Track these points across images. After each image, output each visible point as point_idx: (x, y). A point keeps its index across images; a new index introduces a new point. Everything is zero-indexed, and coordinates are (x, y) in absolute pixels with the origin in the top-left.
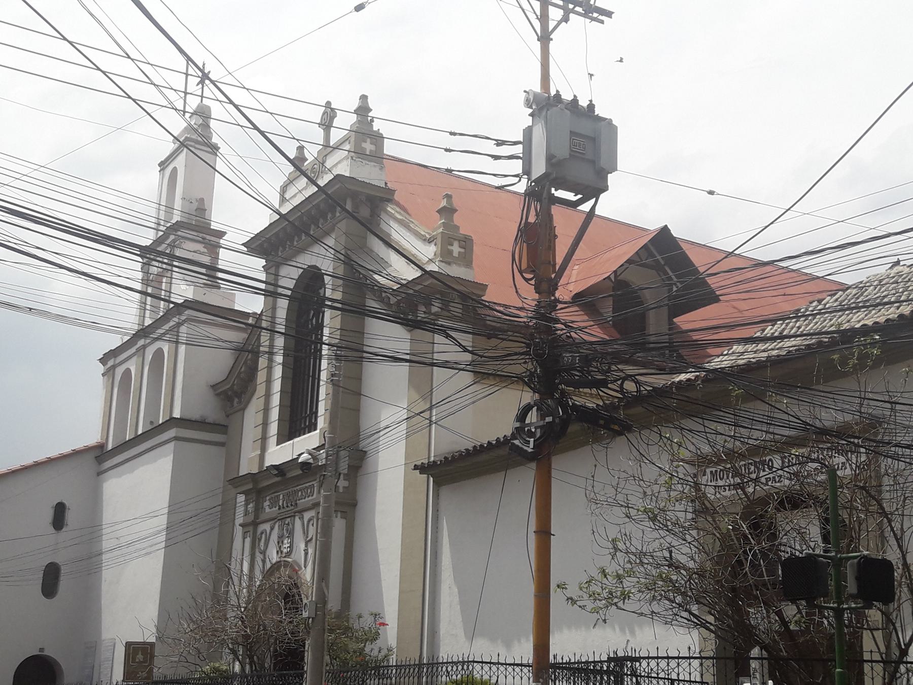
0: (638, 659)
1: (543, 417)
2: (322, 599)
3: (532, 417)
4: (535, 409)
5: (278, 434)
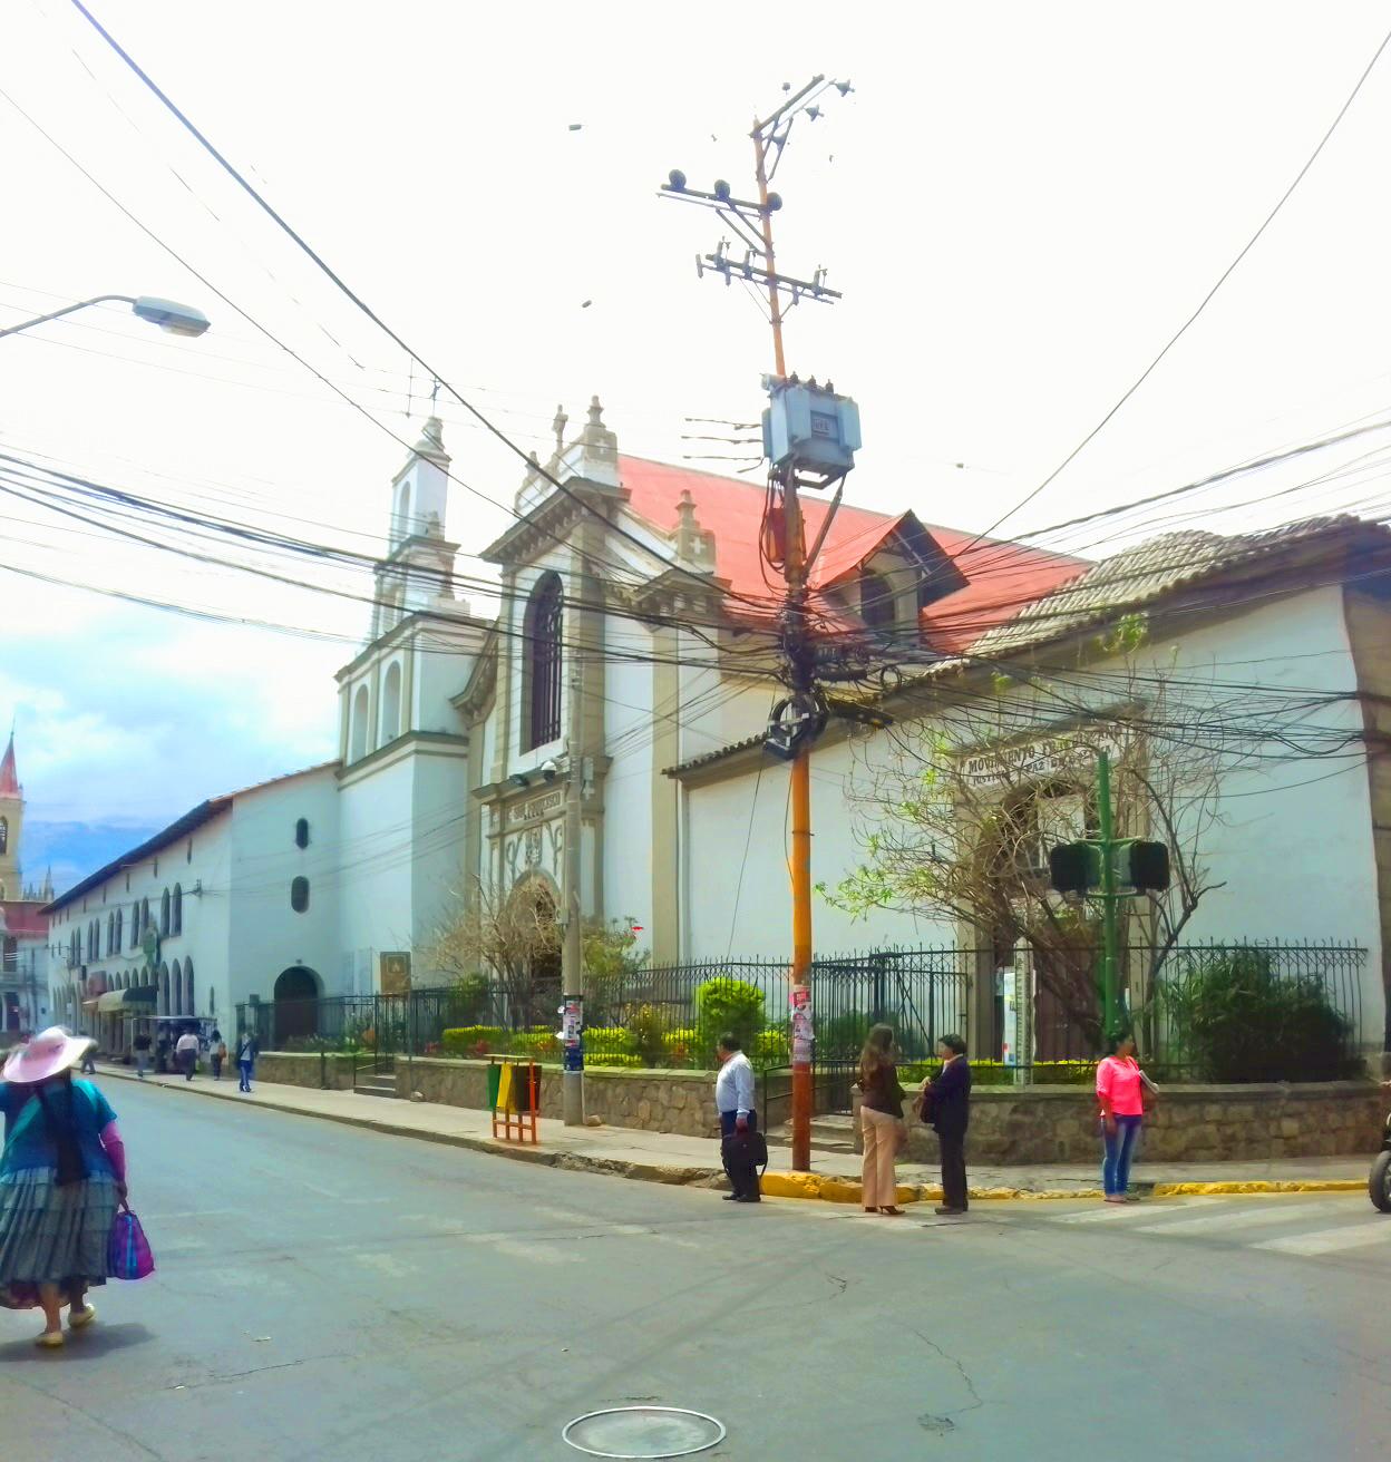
0: (899, 956)
1: (799, 715)
2: (575, 907)
3: (788, 715)
4: (790, 705)
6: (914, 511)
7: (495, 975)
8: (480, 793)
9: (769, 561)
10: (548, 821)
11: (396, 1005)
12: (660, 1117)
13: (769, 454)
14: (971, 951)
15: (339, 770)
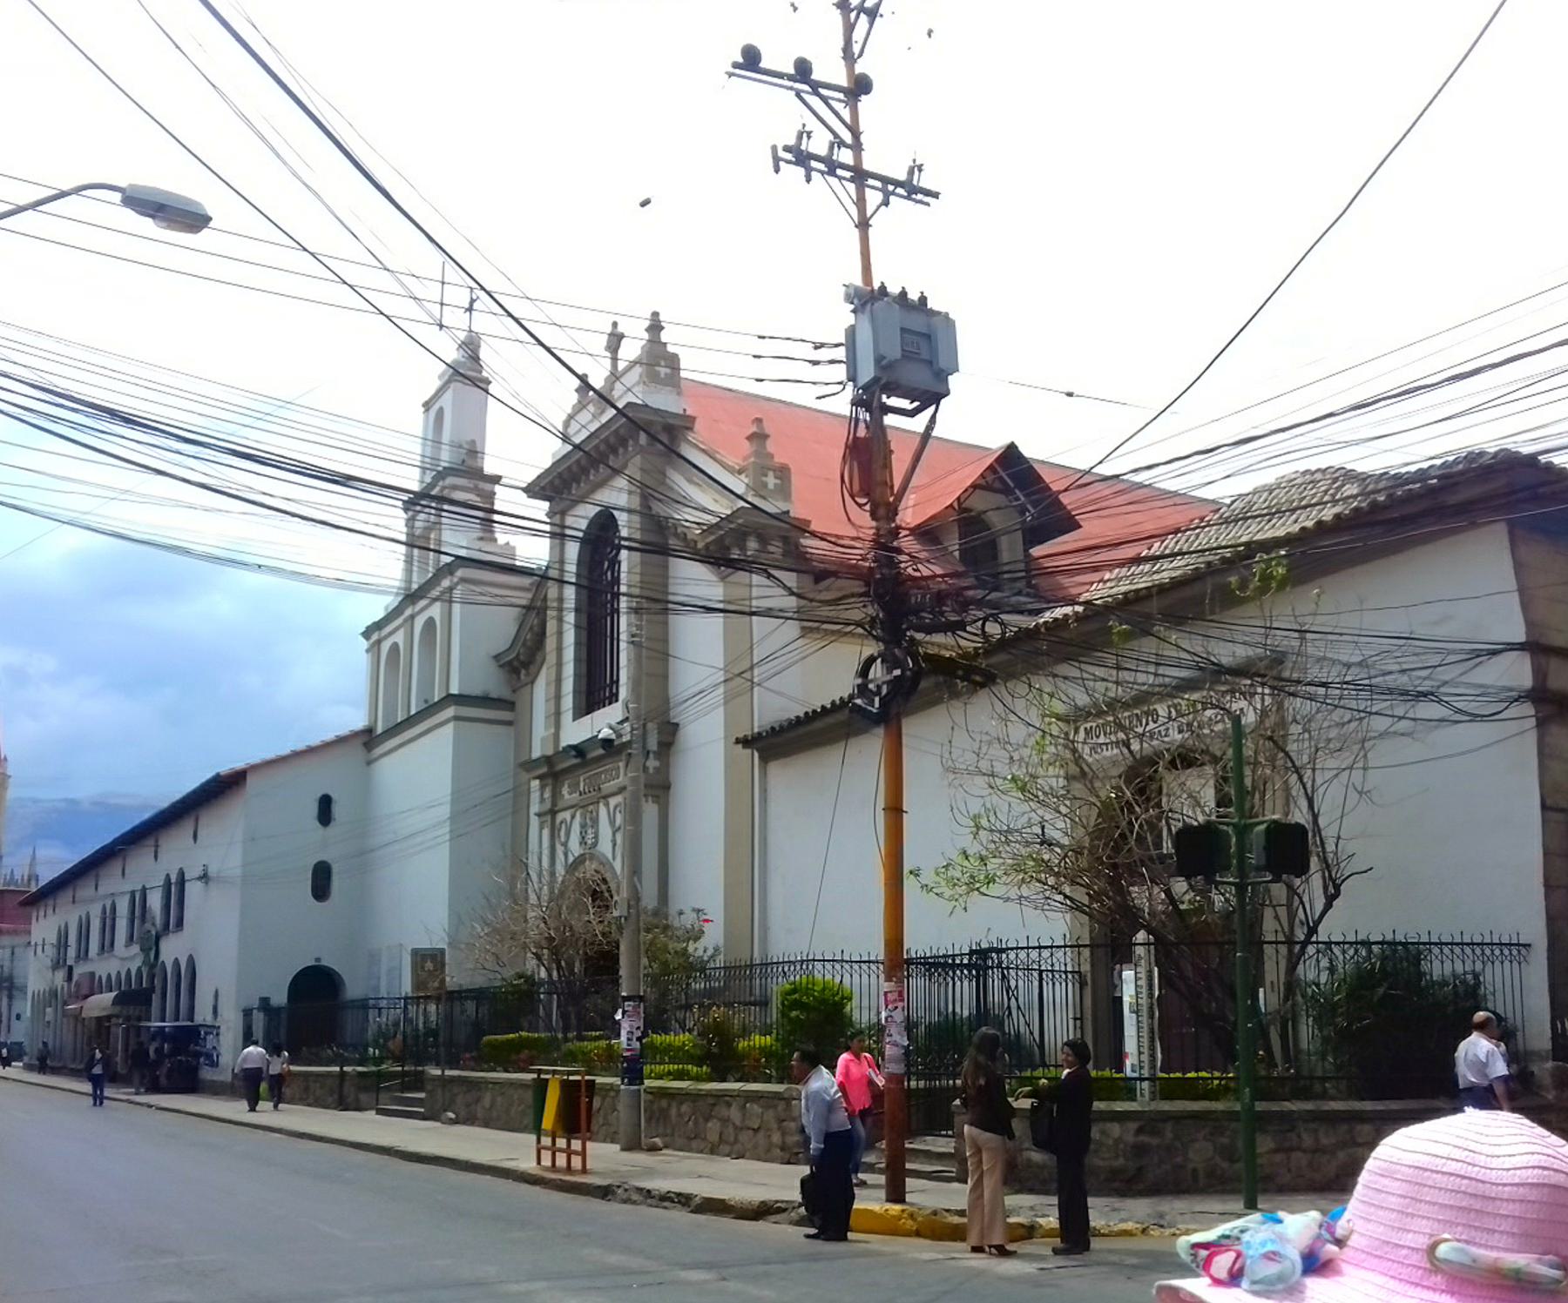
1: (889, 671)
2: (636, 897)
3: (877, 671)
4: (879, 661)
5: (574, 708)
6: (1016, 443)
7: (543, 974)
8: (529, 765)
9: (852, 497)
10: (605, 797)
11: (428, 1007)
12: (732, 1139)
13: (852, 378)
14: (1085, 946)
15: (368, 739)
